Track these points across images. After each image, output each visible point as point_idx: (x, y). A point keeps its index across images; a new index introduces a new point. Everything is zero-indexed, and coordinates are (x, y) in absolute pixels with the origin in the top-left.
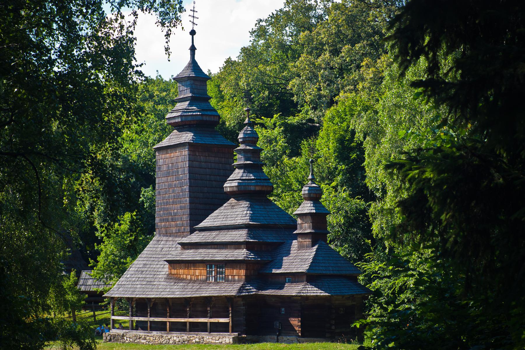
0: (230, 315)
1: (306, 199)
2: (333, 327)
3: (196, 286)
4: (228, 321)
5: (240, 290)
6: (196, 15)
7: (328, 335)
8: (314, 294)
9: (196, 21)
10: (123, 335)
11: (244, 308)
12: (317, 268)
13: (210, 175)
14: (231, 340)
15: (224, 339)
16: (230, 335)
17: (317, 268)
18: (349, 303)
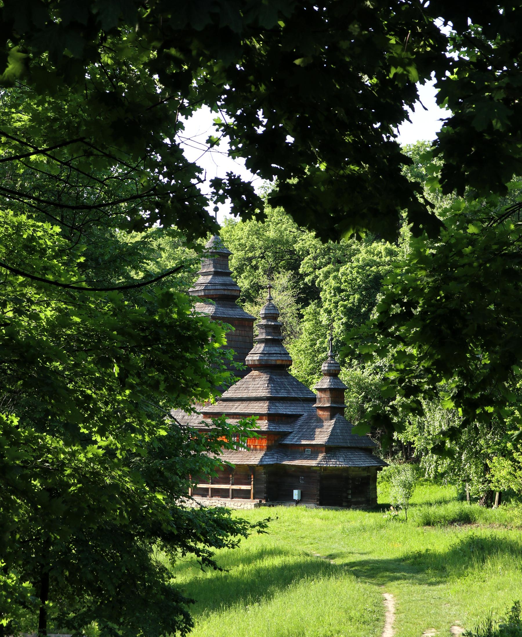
0: (252, 483)
1: (325, 375)
2: (350, 497)
5: (261, 460)
7: (344, 504)
15: (246, 505)
18: (365, 474)
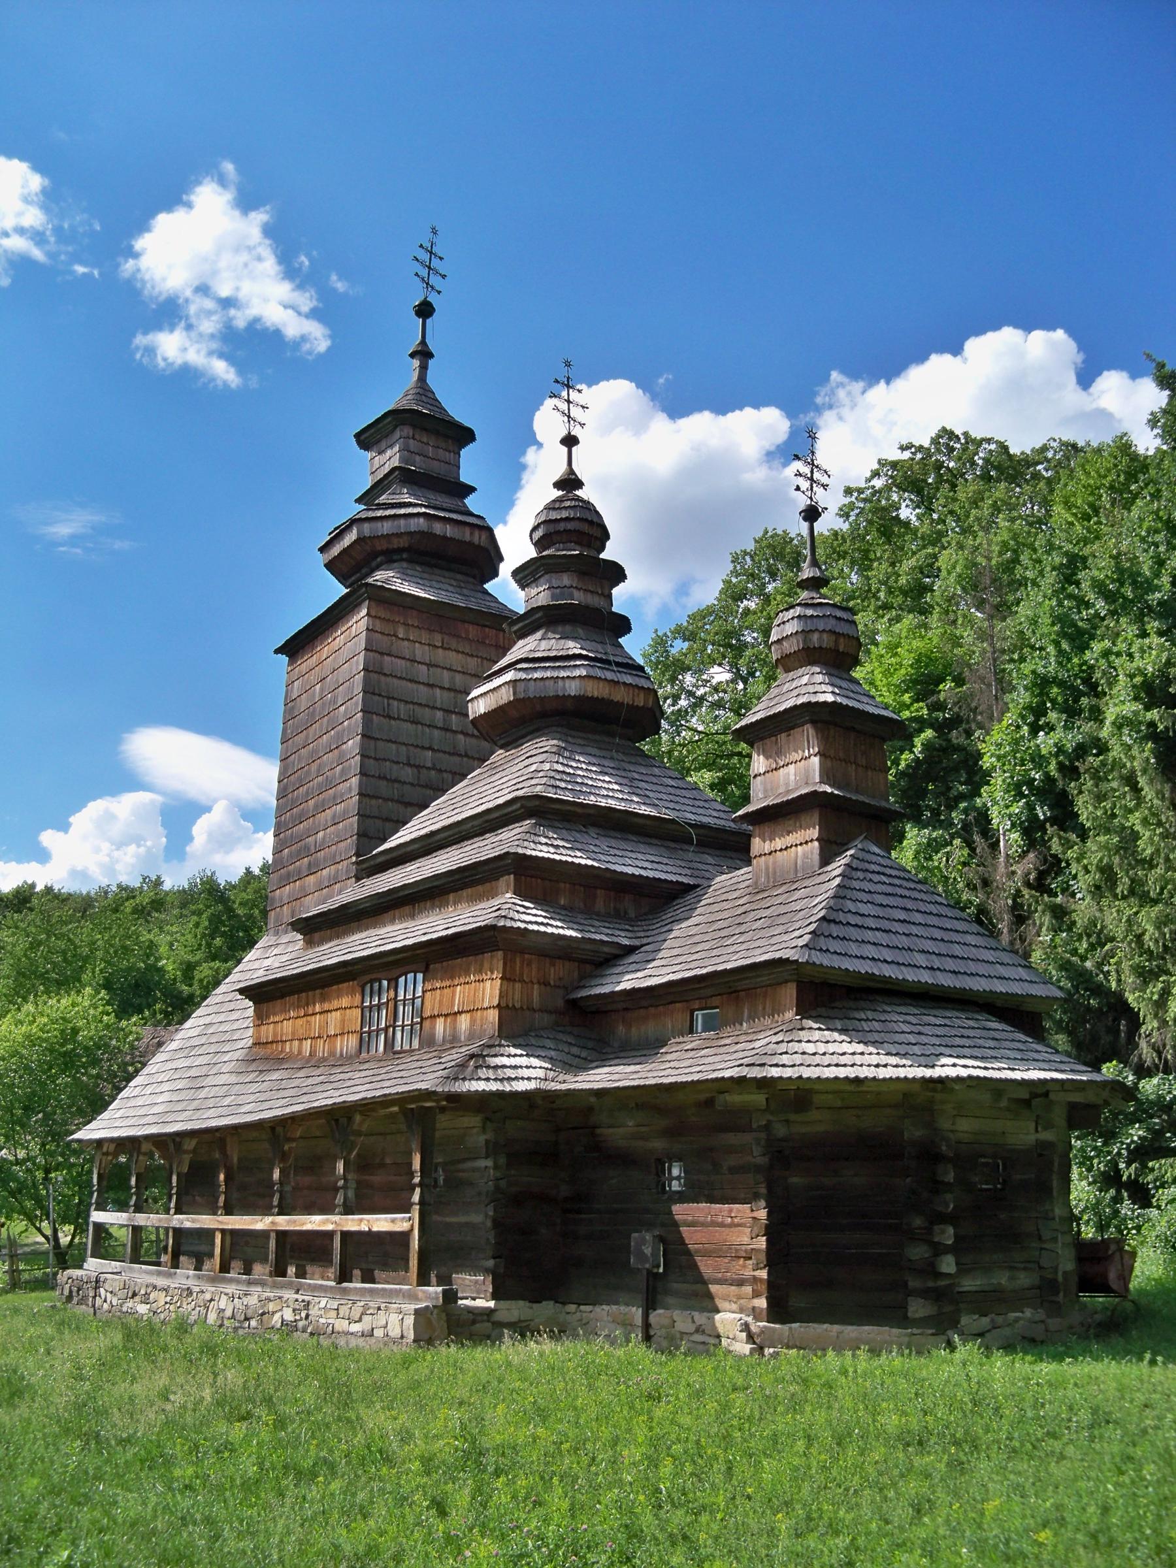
0: (416, 1198)
2: (948, 1265)
3: (317, 1076)
4: (405, 1226)
6: (435, 263)
7: (918, 1308)
8: (842, 1073)
9: (435, 280)
10: (97, 1281)
11: (489, 1163)
12: (854, 949)
13: (447, 711)
14: (410, 1321)
15: (381, 1318)
16: (412, 1297)
17: (854, 949)
18: (1024, 1134)
